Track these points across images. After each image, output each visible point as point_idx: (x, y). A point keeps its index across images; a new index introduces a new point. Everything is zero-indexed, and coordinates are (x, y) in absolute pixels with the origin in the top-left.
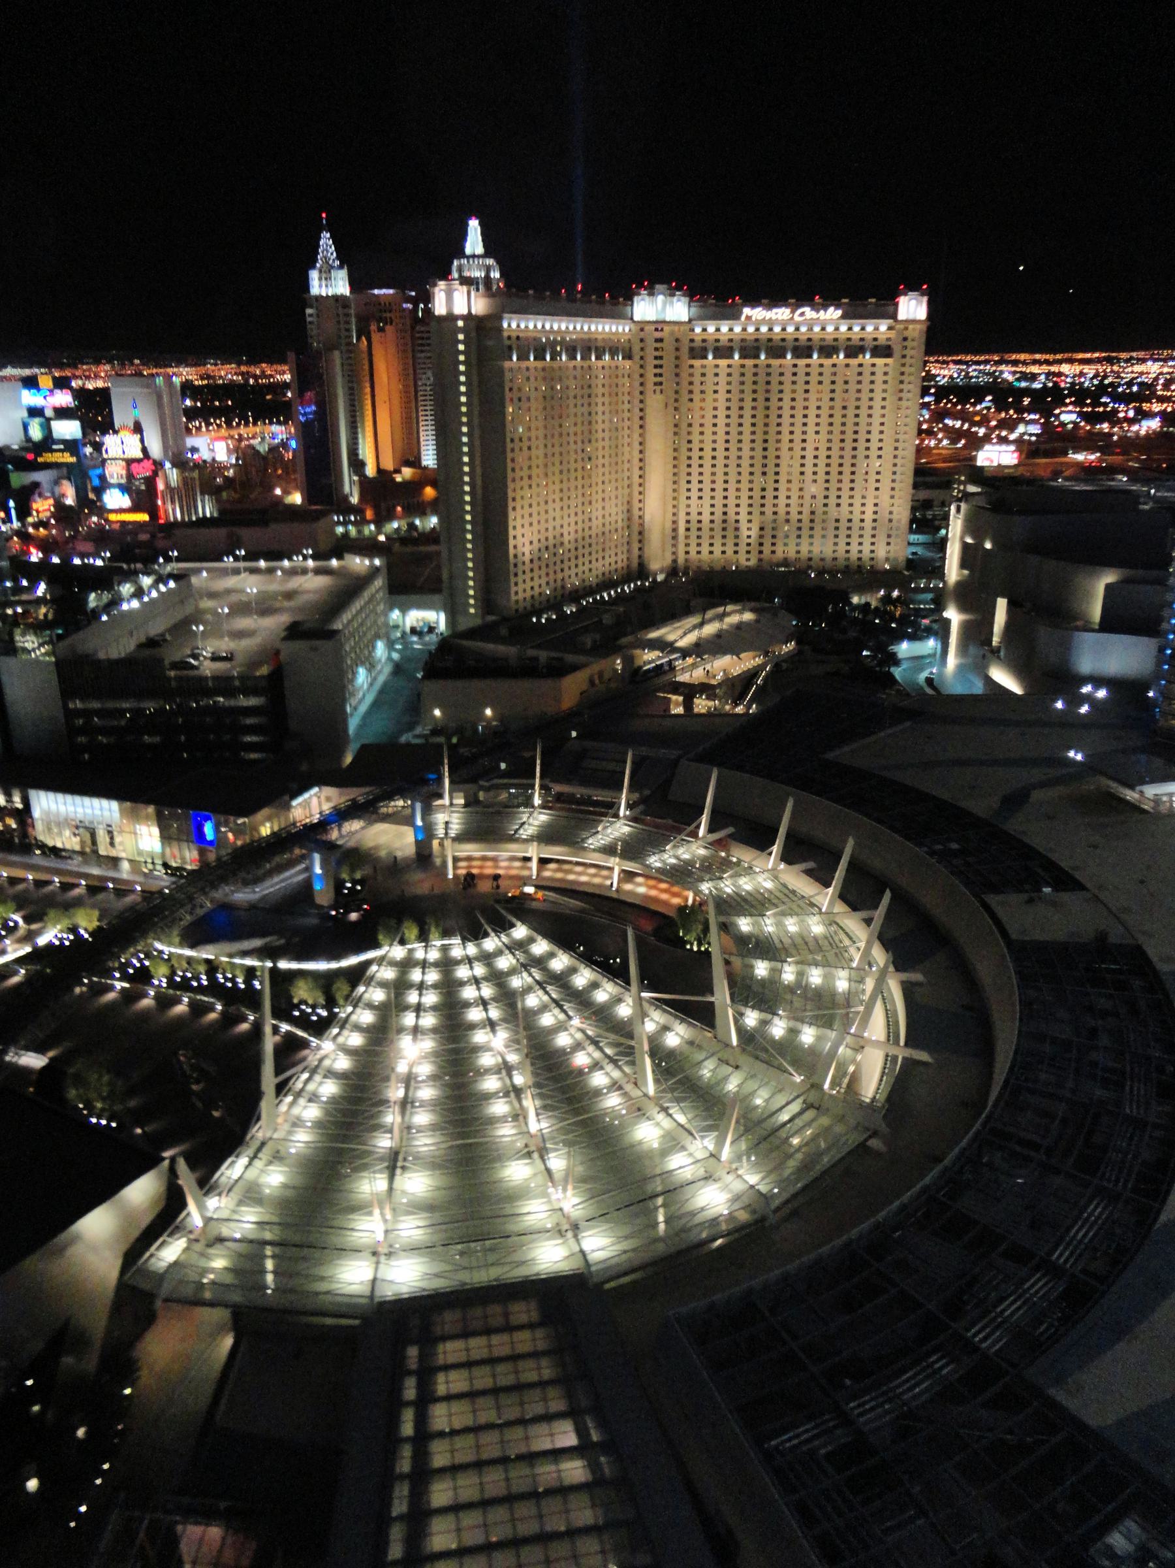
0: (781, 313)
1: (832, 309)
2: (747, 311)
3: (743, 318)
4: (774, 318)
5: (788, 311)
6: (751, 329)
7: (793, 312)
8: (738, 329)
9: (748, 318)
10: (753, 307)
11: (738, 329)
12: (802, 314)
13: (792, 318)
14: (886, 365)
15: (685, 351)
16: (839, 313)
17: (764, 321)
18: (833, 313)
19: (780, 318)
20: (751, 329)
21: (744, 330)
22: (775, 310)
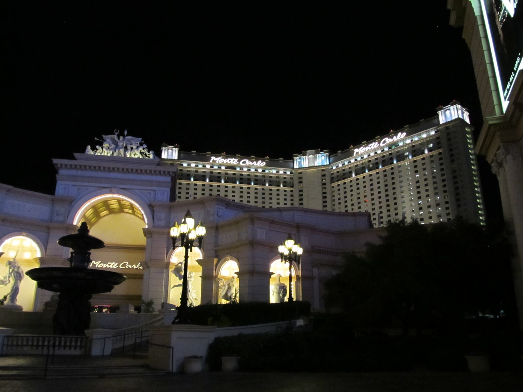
0: (374, 145)
1: (400, 134)
2: (356, 150)
3: (355, 154)
4: (370, 148)
5: (376, 143)
6: (359, 159)
7: (379, 143)
8: (353, 161)
9: (357, 153)
10: (358, 148)
11: (353, 161)
12: (385, 142)
13: (379, 146)
14: (440, 154)
15: (327, 180)
16: (405, 134)
17: (365, 153)
18: (401, 135)
19: (373, 147)
20: (359, 159)
21: (356, 160)
22: (369, 145)
